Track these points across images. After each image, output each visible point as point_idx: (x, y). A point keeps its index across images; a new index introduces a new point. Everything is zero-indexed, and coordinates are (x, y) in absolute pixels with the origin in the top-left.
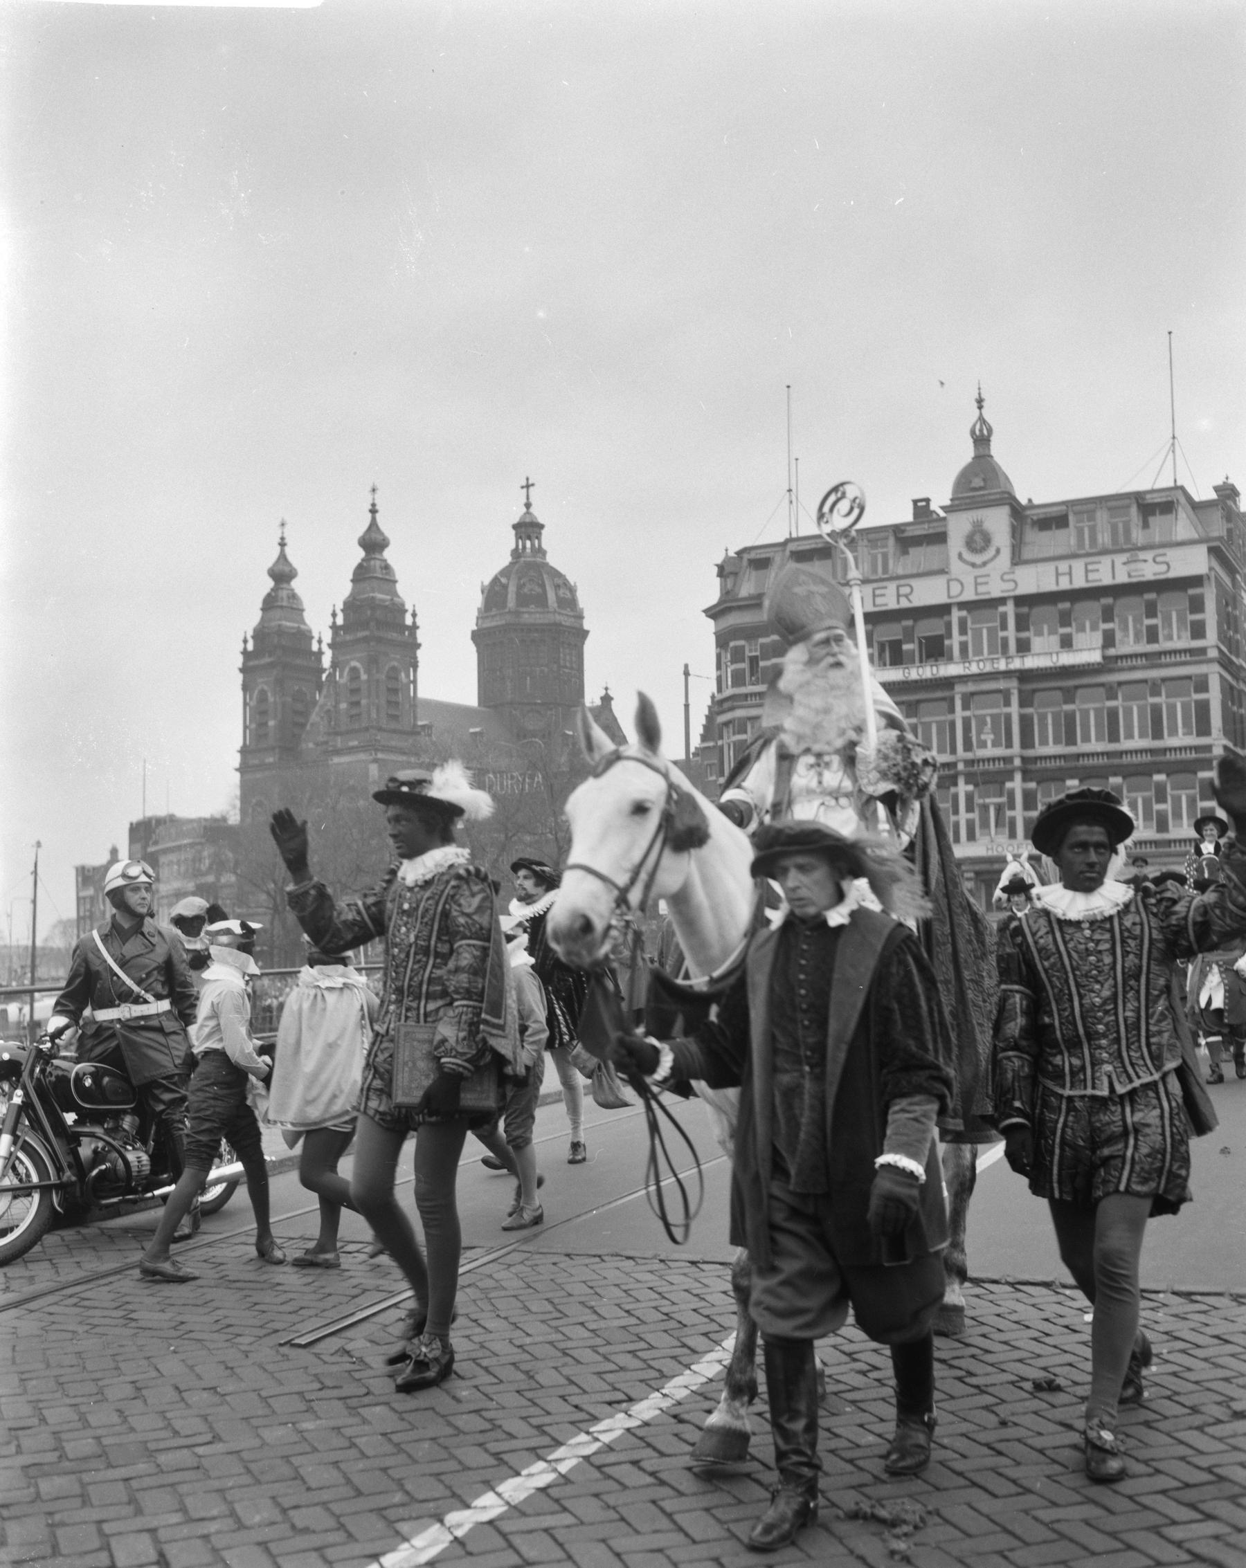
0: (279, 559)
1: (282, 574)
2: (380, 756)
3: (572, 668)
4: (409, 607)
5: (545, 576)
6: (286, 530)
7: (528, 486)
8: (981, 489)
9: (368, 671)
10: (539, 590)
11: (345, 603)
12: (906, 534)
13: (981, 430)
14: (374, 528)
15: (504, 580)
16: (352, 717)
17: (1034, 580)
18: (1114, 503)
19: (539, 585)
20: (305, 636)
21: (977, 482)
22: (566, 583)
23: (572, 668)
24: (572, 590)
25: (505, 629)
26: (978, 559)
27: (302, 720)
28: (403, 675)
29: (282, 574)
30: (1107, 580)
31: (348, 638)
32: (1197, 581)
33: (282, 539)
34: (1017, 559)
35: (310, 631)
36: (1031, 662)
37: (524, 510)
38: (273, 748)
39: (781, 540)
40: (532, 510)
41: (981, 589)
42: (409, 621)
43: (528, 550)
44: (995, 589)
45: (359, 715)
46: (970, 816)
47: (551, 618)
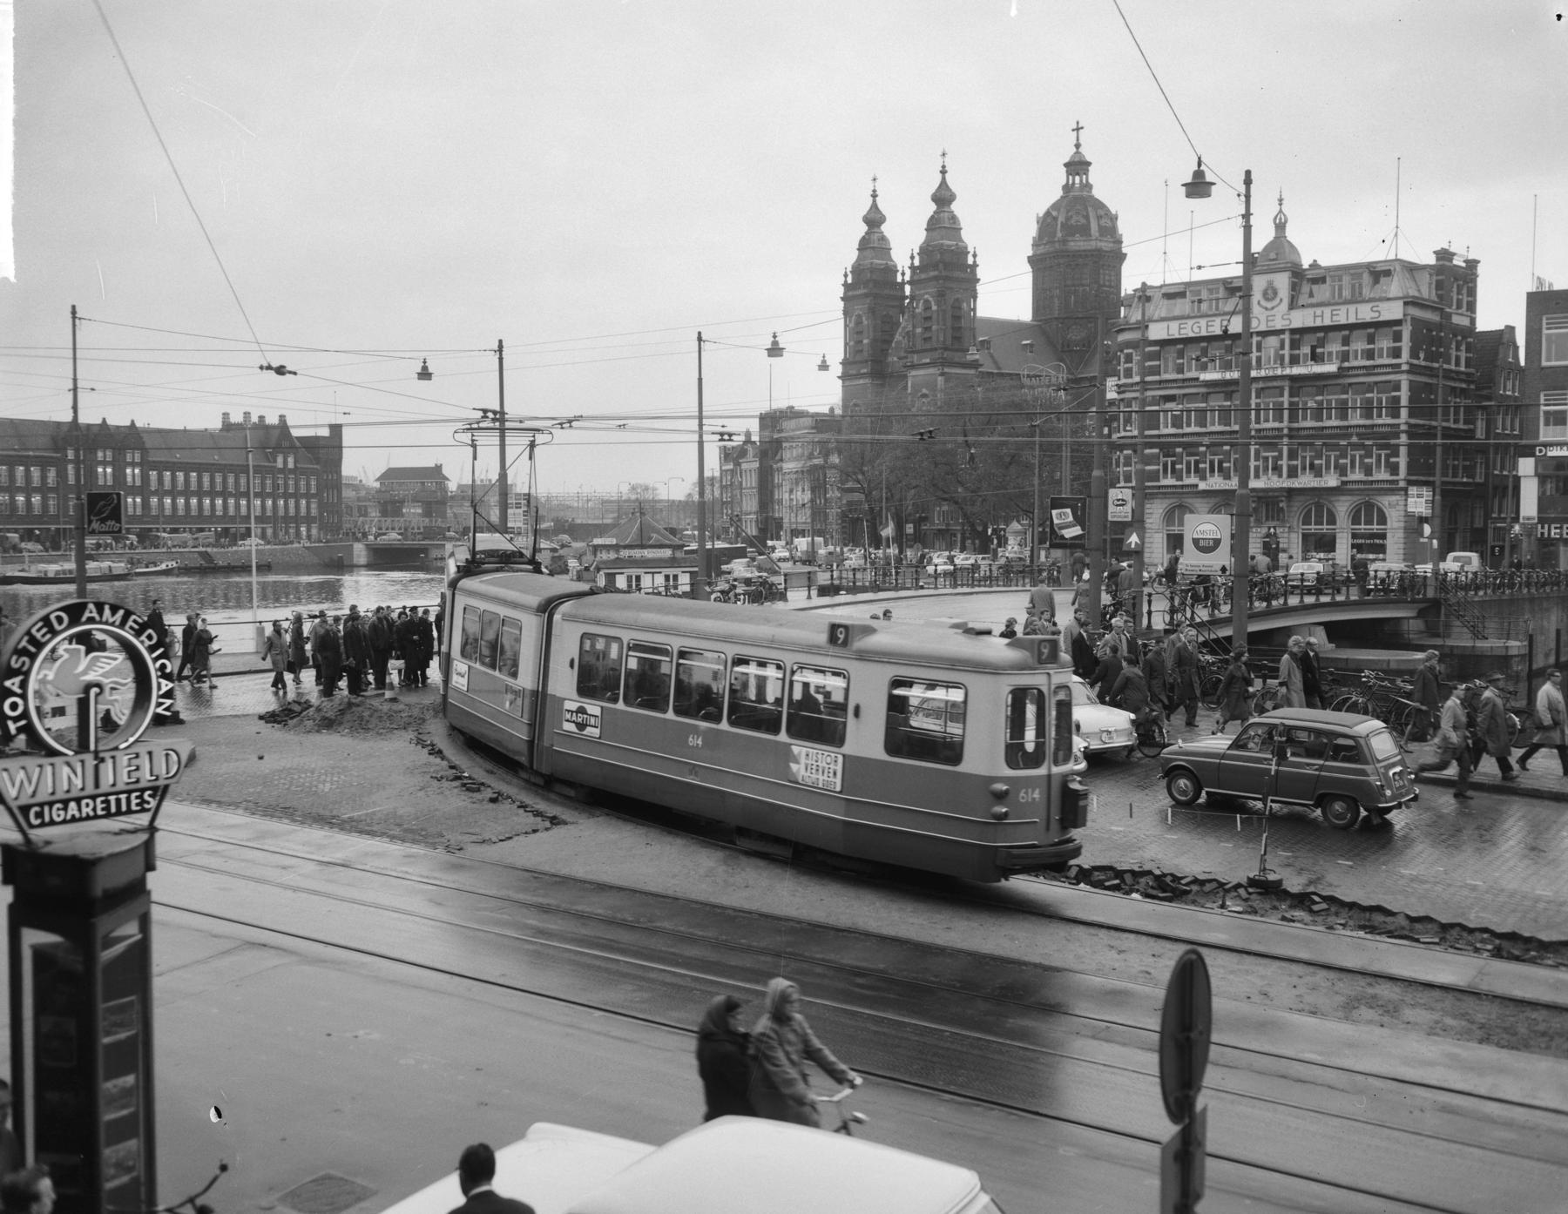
0: (871, 208)
1: (874, 220)
2: (946, 370)
3: (1110, 286)
4: (970, 249)
5: (1090, 209)
7: (1078, 129)
8: (1273, 260)
9: (938, 304)
10: (1083, 221)
11: (921, 248)
12: (1233, 285)
13: (1281, 219)
14: (944, 187)
15: (1054, 213)
16: (925, 339)
17: (1301, 319)
18: (1354, 270)
19: (1083, 216)
20: (891, 270)
21: (1272, 256)
23: (1110, 286)
24: (1114, 218)
26: (1269, 305)
28: (965, 305)
29: (874, 220)
30: (1343, 321)
32: (1398, 322)
34: (1293, 305)
35: (895, 266)
36: (1296, 371)
37: (1075, 150)
38: (867, 361)
40: (1080, 150)
41: (1270, 324)
42: (970, 261)
44: (1278, 324)
45: (930, 338)
46: (1257, 463)
47: (1093, 245)
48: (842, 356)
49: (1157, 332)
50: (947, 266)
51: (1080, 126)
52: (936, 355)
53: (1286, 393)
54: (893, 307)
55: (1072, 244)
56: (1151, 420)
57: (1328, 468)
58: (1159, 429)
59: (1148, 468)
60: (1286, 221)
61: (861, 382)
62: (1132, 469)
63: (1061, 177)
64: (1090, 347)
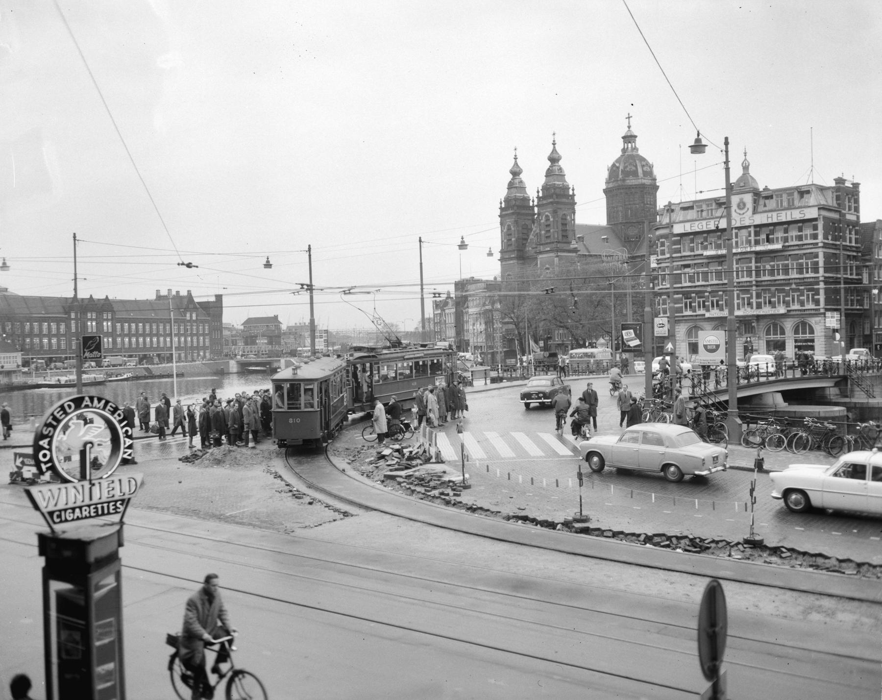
1: (516, 173)
4: (571, 186)
5: (637, 162)
6: (517, 152)
7: (629, 118)
9: (553, 217)
10: (634, 168)
11: (543, 187)
12: (720, 201)
14: (554, 152)
15: (617, 165)
16: (547, 237)
17: (760, 219)
18: (789, 191)
19: (634, 166)
20: (526, 199)
21: (742, 184)
22: (648, 164)
24: (651, 167)
25: (619, 188)
26: (742, 212)
27: (526, 237)
28: (569, 217)
29: (516, 173)
30: (784, 220)
31: (545, 202)
32: (815, 219)
33: (516, 156)
34: (755, 211)
36: (759, 248)
37: (627, 129)
38: (514, 250)
39: (678, 202)
40: (631, 129)
41: (742, 222)
42: (571, 192)
43: (630, 149)
44: (747, 223)
46: (738, 301)
47: (640, 181)
48: (500, 248)
49: (678, 229)
50: (558, 196)
51: (630, 115)
52: (554, 245)
53: (753, 261)
54: (529, 220)
55: (628, 181)
56: (677, 278)
57: (779, 302)
58: (681, 283)
59: (676, 306)
60: (749, 165)
61: (512, 262)
62: (667, 306)
63: (620, 144)
64: (640, 238)
